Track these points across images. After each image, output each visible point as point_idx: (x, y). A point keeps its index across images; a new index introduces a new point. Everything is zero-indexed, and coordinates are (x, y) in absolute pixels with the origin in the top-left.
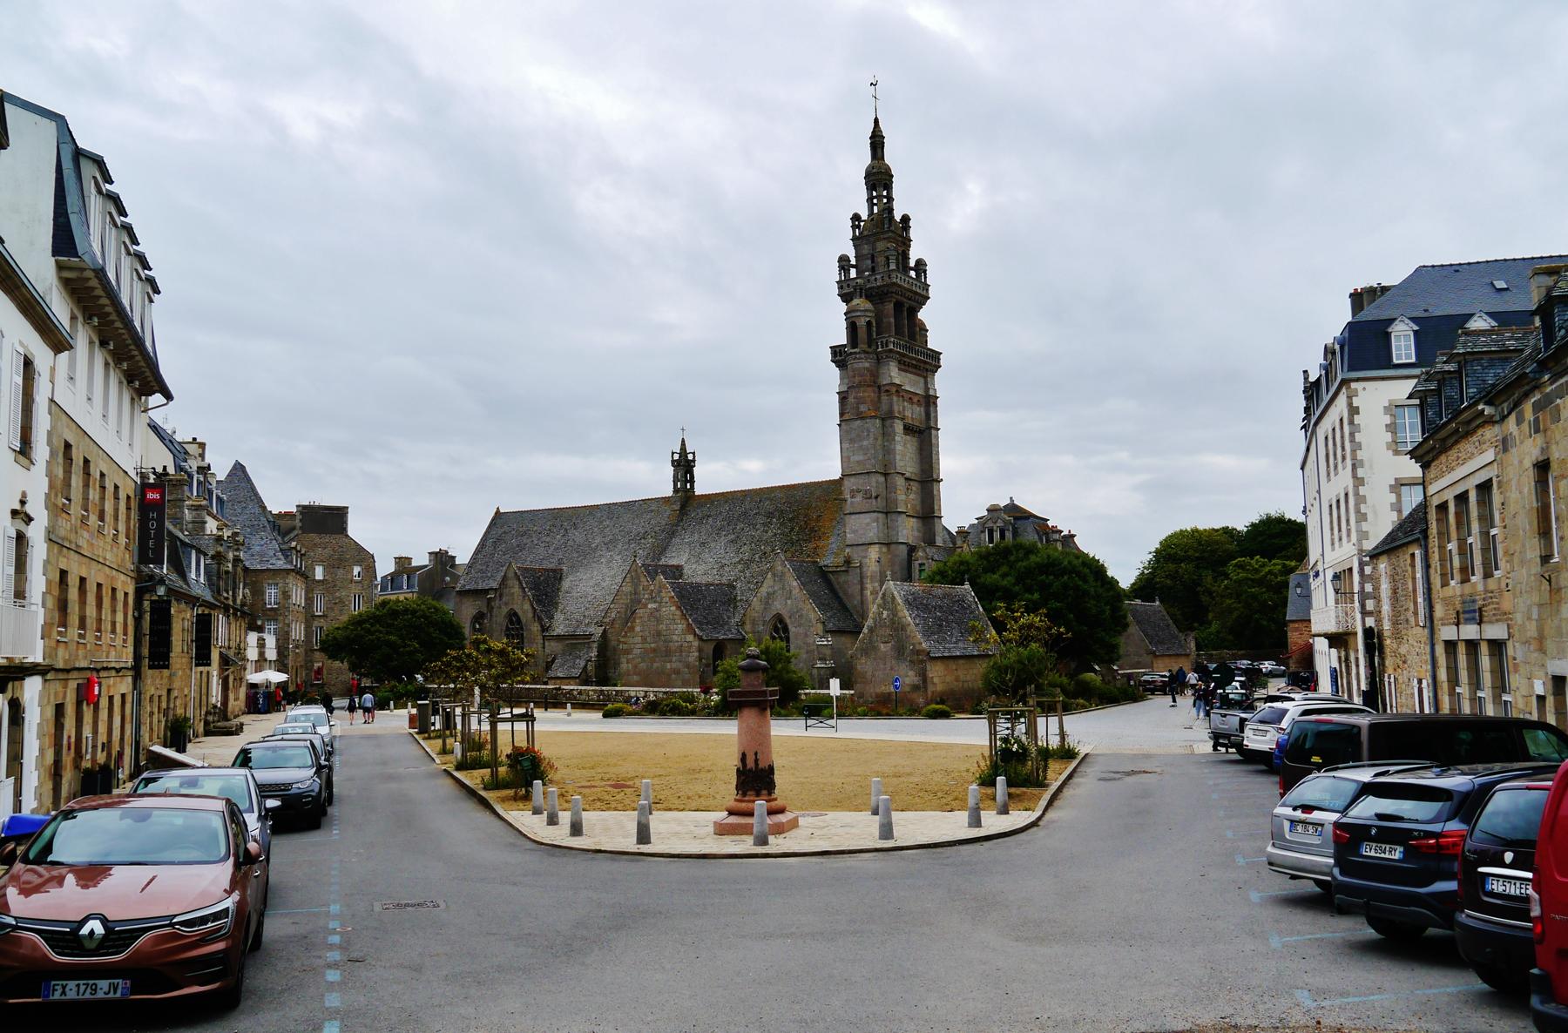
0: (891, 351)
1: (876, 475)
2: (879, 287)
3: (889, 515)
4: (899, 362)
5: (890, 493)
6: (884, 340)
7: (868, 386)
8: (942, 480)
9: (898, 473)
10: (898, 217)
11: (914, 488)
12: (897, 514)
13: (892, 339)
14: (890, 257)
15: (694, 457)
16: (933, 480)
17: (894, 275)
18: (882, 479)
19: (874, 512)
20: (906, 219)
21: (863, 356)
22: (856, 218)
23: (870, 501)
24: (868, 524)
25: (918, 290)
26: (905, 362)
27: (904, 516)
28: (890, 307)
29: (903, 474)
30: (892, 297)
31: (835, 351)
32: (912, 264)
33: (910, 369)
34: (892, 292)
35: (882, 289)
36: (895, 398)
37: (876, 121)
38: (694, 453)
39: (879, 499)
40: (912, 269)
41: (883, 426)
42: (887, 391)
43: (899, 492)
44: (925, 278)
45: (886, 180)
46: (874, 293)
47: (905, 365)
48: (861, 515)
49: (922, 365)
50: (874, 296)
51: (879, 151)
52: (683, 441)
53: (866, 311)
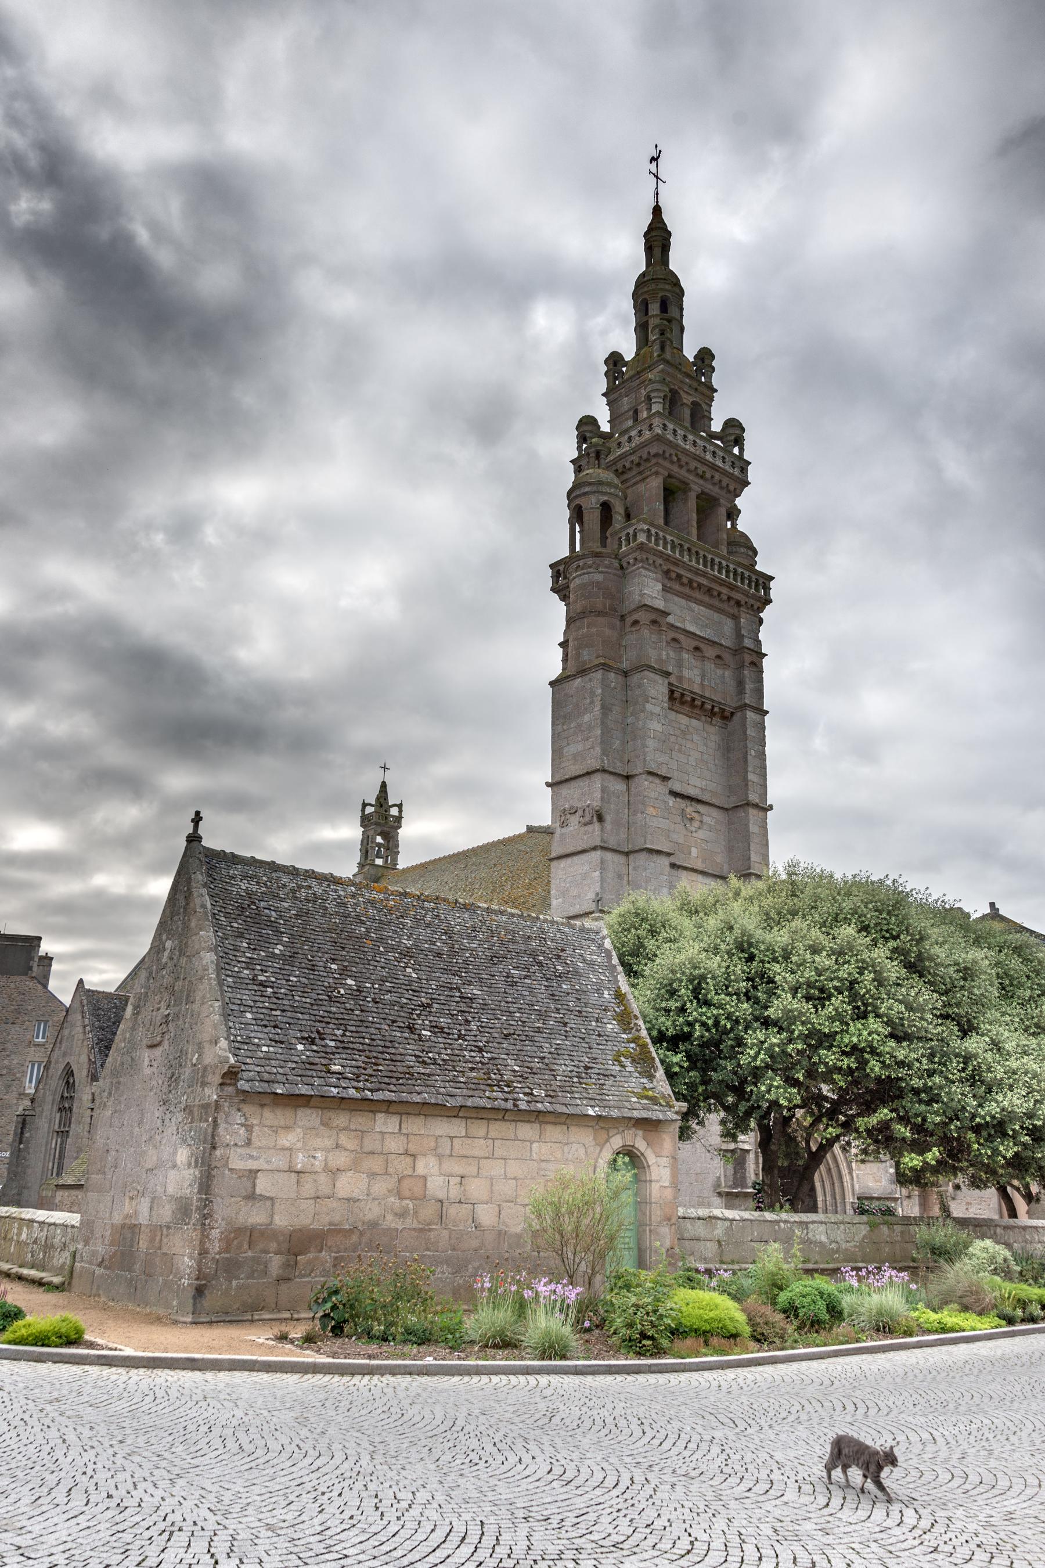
0: (641, 547)
1: (607, 776)
2: (633, 452)
3: (631, 857)
4: (667, 573)
5: (635, 813)
6: (631, 533)
7: (600, 613)
8: (771, 808)
9: (650, 773)
10: (690, 352)
11: (706, 819)
12: (643, 856)
13: (646, 527)
14: (653, 395)
15: (400, 811)
16: (748, 804)
17: (656, 421)
18: (619, 786)
19: (595, 848)
20: (705, 356)
21: (590, 561)
22: (614, 360)
23: (590, 828)
24: (585, 876)
25: (720, 463)
26: (679, 577)
27: (665, 861)
28: (655, 484)
29: (665, 779)
30: (657, 464)
31: (558, 571)
32: (716, 426)
33: (697, 595)
34: (656, 455)
35: (638, 454)
36: (646, 633)
37: (657, 211)
38: (400, 806)
39: (608, 825)
40: (713, 436)
41: (626, 687)
42: (636, 623)
43: (651, 811)
44: (742, 450)
45: (661, 289)
46: (628, 465)
47: (682, 584)
48: (575, 858)
49: (725, 591)
50: (630, 469)
51: (657, 252)
52: (384, 785)
53: (600, 483)
